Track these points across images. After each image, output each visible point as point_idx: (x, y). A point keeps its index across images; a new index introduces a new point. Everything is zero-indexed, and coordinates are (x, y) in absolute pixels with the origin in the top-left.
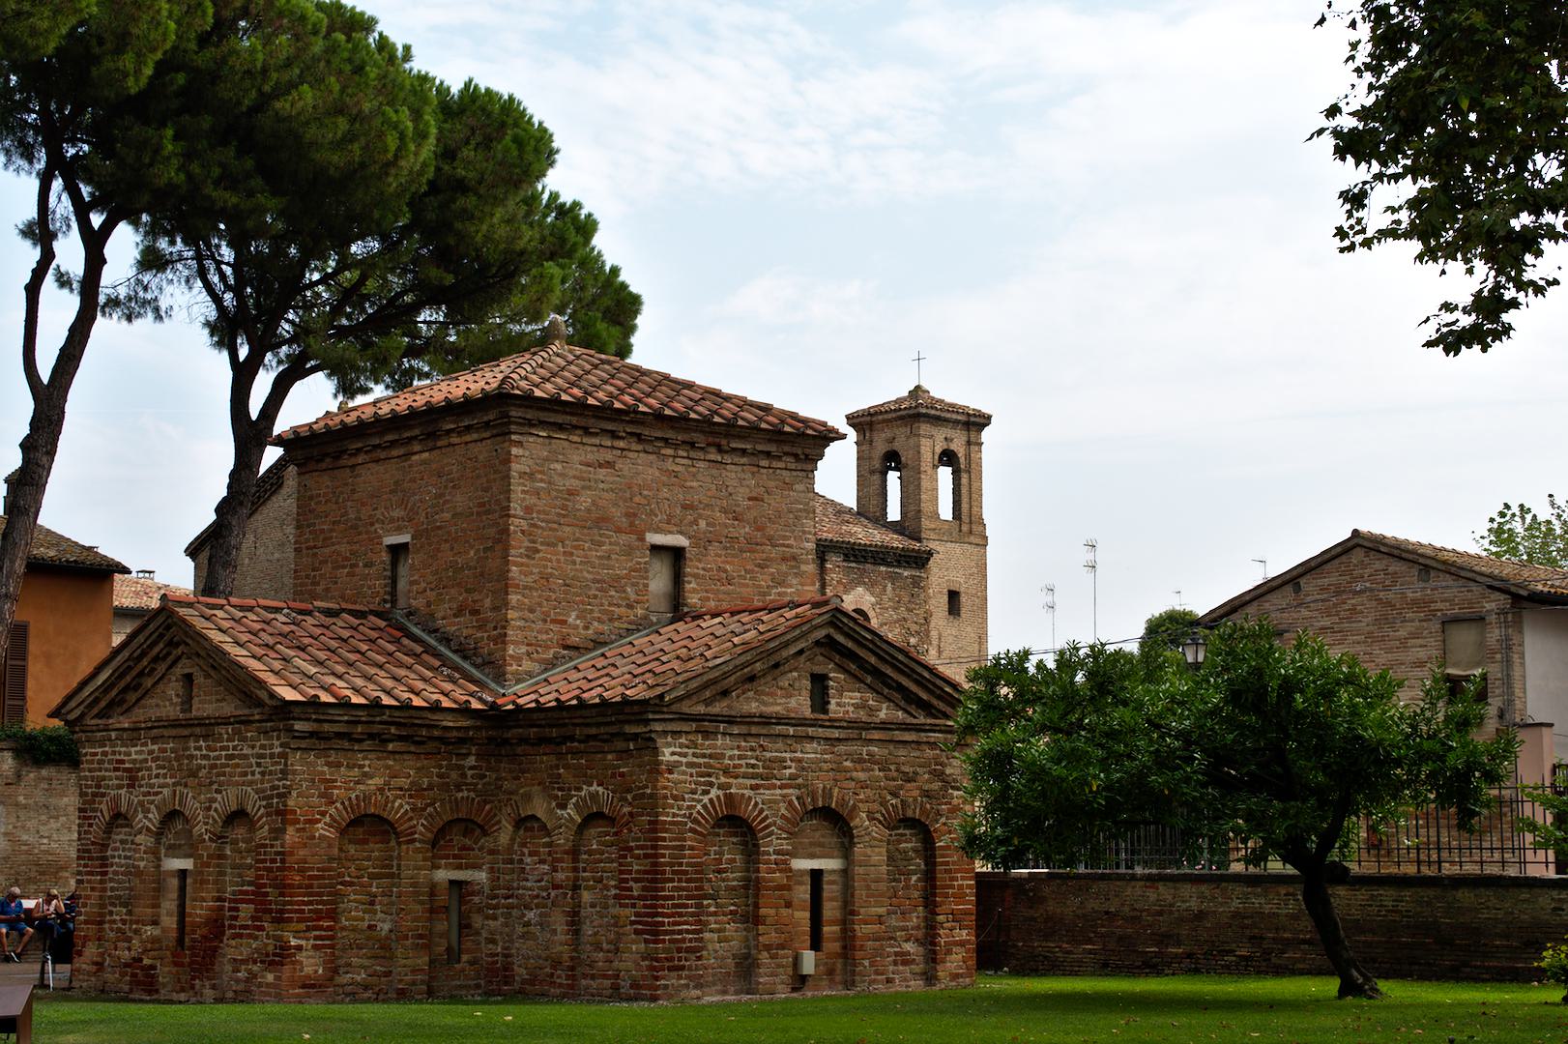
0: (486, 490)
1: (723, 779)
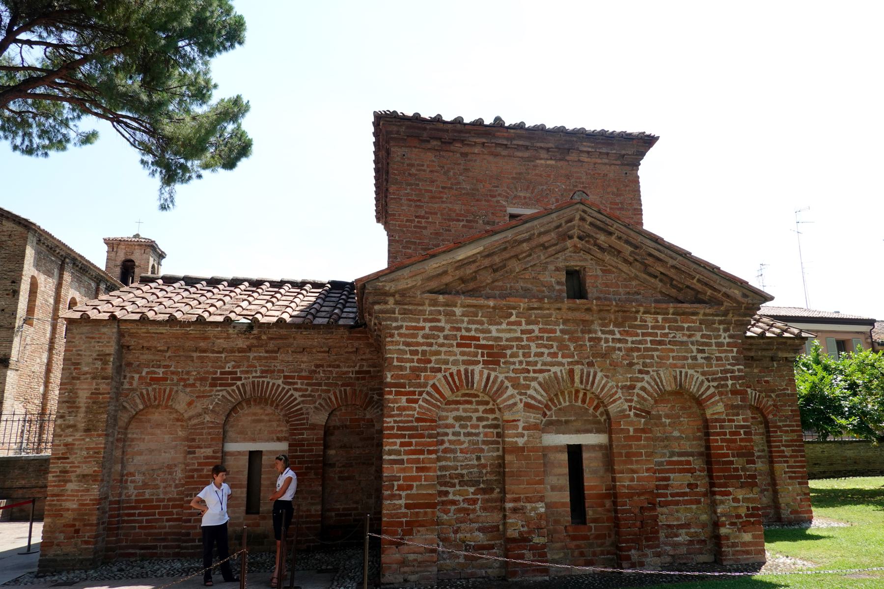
0: (617, 195)
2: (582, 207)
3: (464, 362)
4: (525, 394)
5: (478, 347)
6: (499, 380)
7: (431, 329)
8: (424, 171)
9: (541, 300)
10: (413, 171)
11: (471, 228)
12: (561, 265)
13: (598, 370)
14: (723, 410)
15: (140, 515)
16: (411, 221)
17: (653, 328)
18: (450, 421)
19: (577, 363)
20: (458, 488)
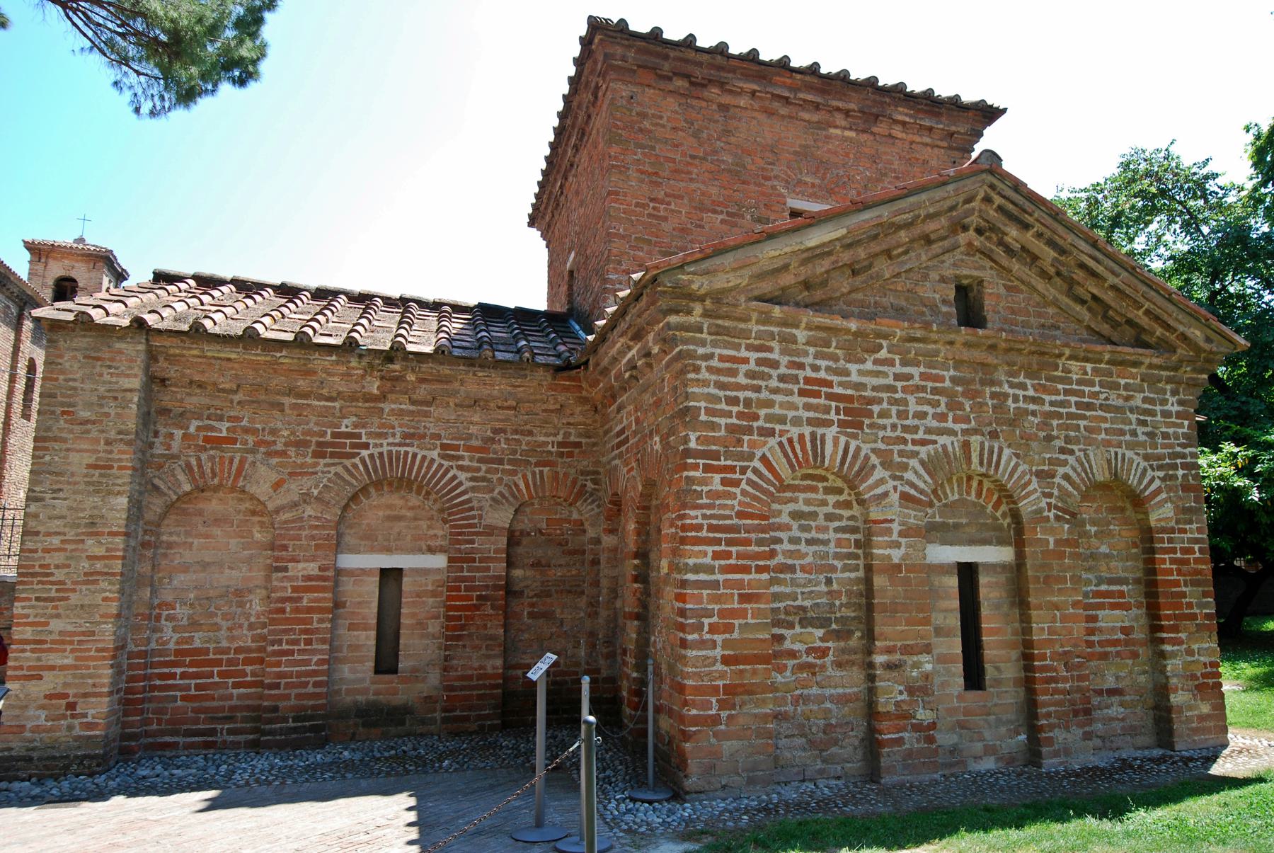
2: (990, 178)
3: (810, 422)
4: (901, 478)
5: (831, 397)
6: (862, 454)
7: (760, 362)
8: (663, 126)
9: (927, 326)
10: (646, 124)
11: (734, 225)
12: (949, 273)
13: (1005, 445)
14: (1171, 514)
15: (184, 676)
16: (644, 206)
17: (1079, 382)
18: (785, 519)
19: (975, 432)
20: (798, 629)
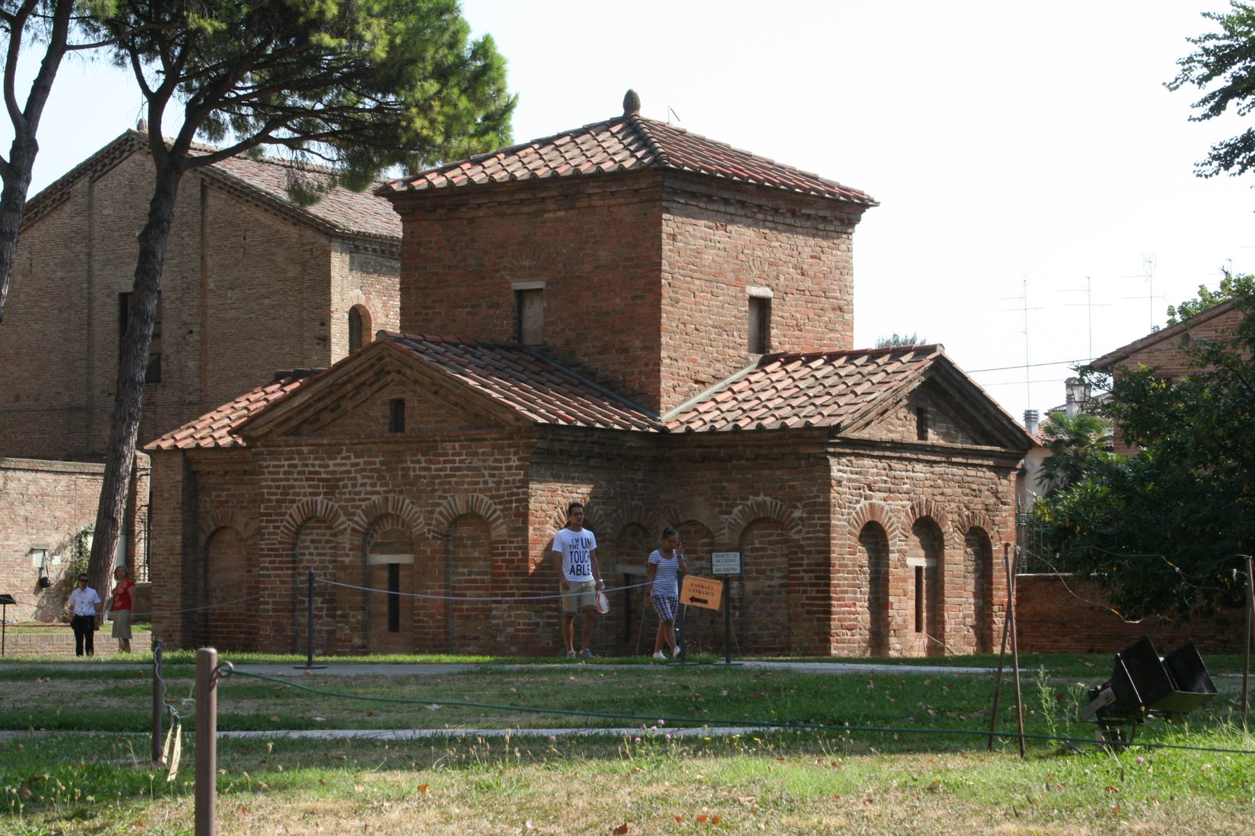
1: (868, 492)
3: (313, 494)
7: (290, 466)
10: (422, 250)
15: (222, 627)
18: (308, 544)
19: (391, 491)
